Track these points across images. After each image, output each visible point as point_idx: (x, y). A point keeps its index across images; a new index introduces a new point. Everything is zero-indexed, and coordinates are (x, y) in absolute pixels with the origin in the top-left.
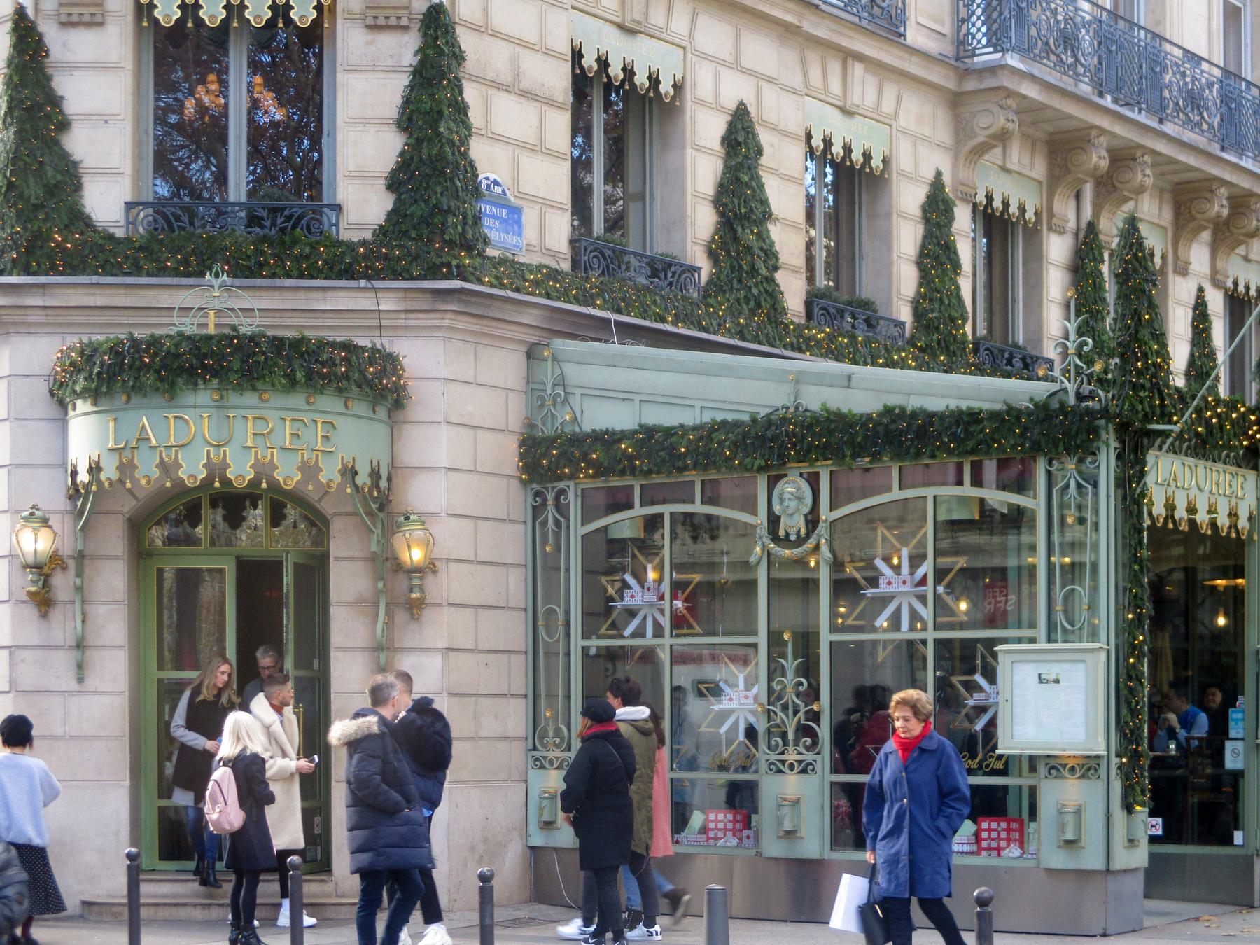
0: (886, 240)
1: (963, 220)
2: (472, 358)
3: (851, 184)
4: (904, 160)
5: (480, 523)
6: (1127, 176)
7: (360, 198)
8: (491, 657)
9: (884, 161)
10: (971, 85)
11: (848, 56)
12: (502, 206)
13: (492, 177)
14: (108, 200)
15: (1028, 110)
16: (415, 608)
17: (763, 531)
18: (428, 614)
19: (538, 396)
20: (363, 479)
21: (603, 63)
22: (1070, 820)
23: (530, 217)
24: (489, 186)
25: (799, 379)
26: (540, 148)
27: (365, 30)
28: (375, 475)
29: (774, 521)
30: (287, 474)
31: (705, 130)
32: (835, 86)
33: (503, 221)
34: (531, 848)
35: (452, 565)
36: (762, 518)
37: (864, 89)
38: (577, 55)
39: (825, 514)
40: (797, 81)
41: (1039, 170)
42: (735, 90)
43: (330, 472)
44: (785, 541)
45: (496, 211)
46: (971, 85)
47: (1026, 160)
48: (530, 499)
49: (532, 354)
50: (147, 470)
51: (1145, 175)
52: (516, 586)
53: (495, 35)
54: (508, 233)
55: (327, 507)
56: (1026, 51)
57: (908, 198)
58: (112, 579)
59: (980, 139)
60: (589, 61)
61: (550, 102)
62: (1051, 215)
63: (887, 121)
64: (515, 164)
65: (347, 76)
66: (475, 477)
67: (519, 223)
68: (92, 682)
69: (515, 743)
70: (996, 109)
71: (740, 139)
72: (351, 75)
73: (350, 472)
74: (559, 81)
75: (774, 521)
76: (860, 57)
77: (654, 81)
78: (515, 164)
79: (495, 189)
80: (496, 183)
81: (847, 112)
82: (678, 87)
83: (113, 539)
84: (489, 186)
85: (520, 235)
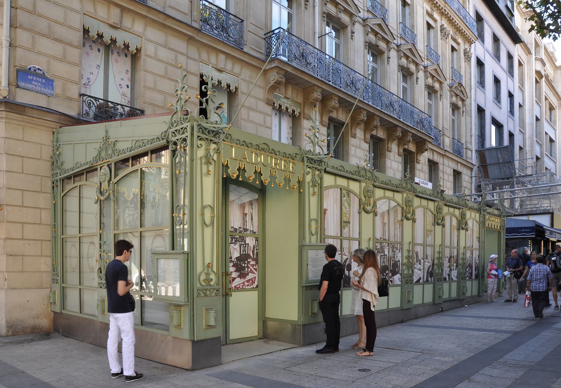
2: (22, 131)
6: (330, 103)
9: (236, 88)
12: (42, 78)
13: (37, 67)
24: (35, 70)
33: (42, 83)
40: (196, 56)
41: (300, 99)
47: (295, 96)
53: (40, 15)
59: (272, 84)
61: (71, 45)
62: (304, 113)
63: (238, 76)
64: (49, 64)
67: (52, 86)
70: (276, 74)
74: (77, 37)
78: (49, 64)
80: (39, 69)
81: (220, 71)
84: (35, 70)
85: (52, 90)
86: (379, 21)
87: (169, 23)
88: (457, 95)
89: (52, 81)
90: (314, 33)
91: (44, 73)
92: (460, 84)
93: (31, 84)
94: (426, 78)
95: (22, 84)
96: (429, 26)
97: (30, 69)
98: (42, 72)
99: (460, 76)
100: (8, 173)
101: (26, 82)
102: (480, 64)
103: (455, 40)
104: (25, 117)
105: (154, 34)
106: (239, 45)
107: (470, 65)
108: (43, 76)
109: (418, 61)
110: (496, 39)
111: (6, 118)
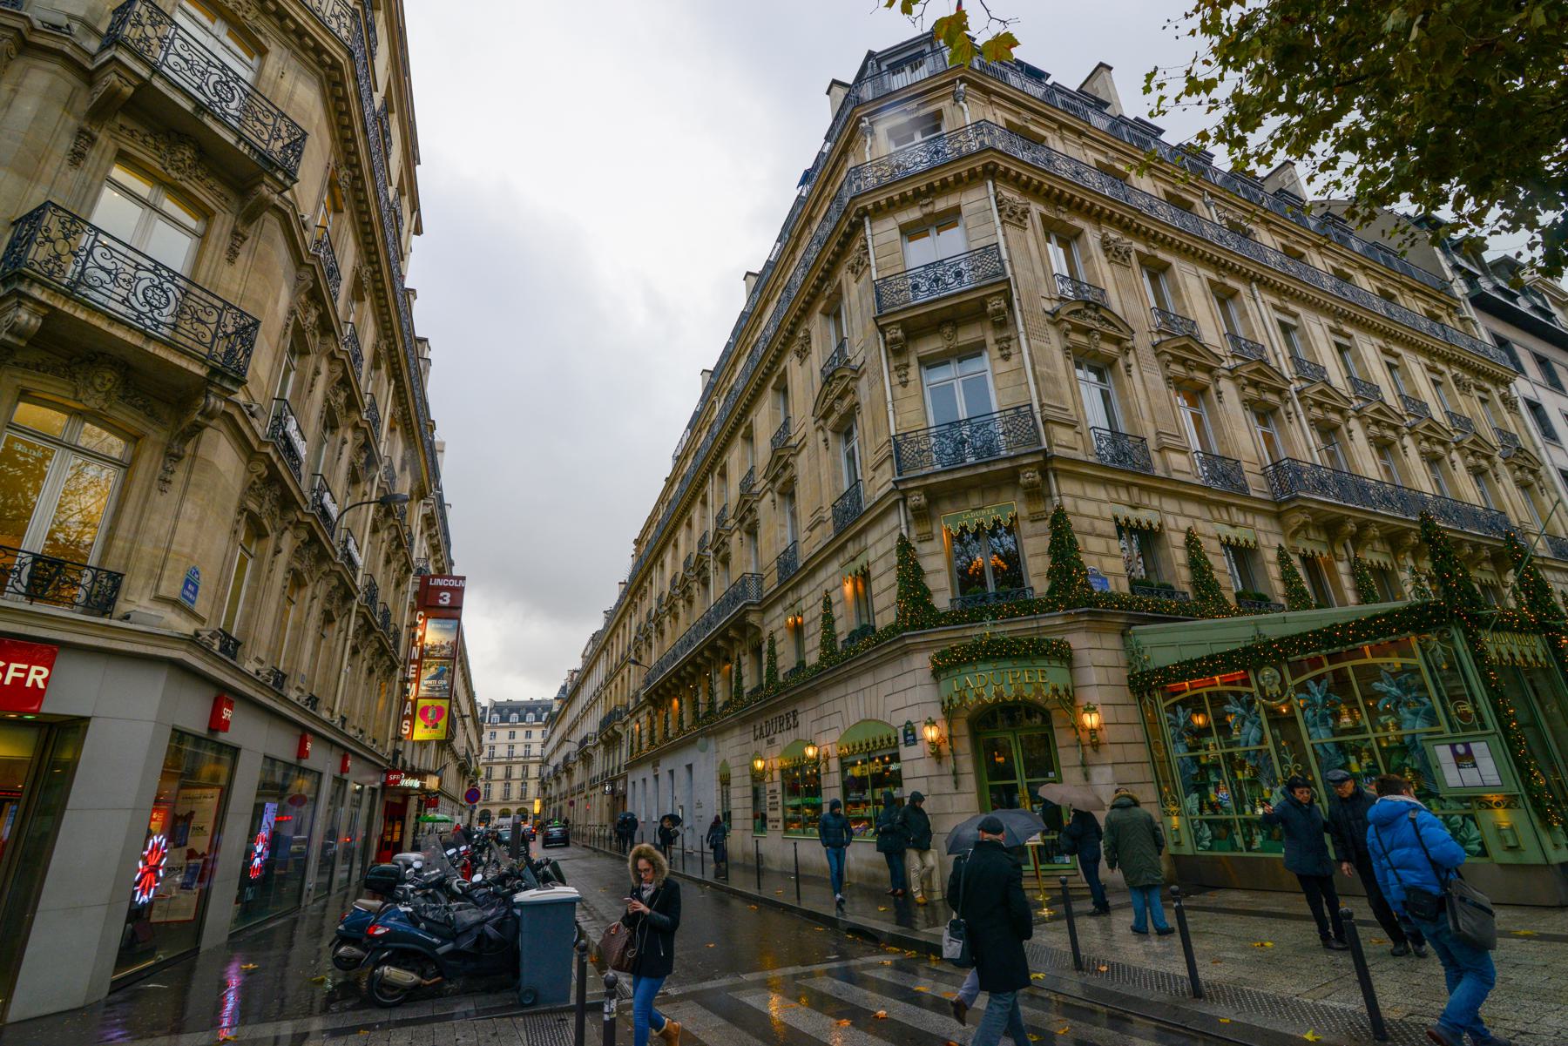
0: (1265, 572)
1: (1296, 561)
3: (1243, 555)
4: (1263, 540)
7: (1038, 585)
10: (1285, 508)
11: (1227, 506)
14: (942, 601)
15: (1313, 512)
17: (1257, 695)
19: (1133, 653)
20: (1062, 692)
21: (1127, 520)
22: (1508, 833)
23: (1111, 580)
25: (1256, 624)
26: (1109, 555)
28: (1067, 690)
29: (1262, 690)
30: (1029, 693)
31: (1178, 539)
32: (1226, 517)
36: (1254, 689)
37: (1238, 517)
38: (1116, 519)
39: (1290, 682)
40: (1208, 517)
42: (1184, 523)
43: (1047, 691)
44: (1271, 698)
46: (1285, 508)
49: (1123, 634)
50: (971, 698)
51: (1374, 531)
52: (1138, 733)
55: (1048, 706)
56: (1307, 490)
57: (1271, 555)
58: (965, 746)
60: (1122, 520)
61: (1109, 537)
63: (1252, 527)
68: (961, 789)
71: (1192, 542)
73: (1056, 690)
74: (1110, 528)
75: (1262, 690)
76: (1233, 505)
77: (1150, 524)
81: (1234, 526)
82: (1160, 525)
83: (962, 728)
86: (1376, 406)
87: (1181, 489)
88: (1521, 468)
90: (1310, 449)
92: (1520, 450)
94: (1464, 458)
96: (1436, 384)
99: (1514, 438)
102: (1535, 407)
103: (1479, 388)
105: (1170, 505)
106: (1243, 490)
107: (1522, 417)
109: (1446, 437)
110: (1542, 362)
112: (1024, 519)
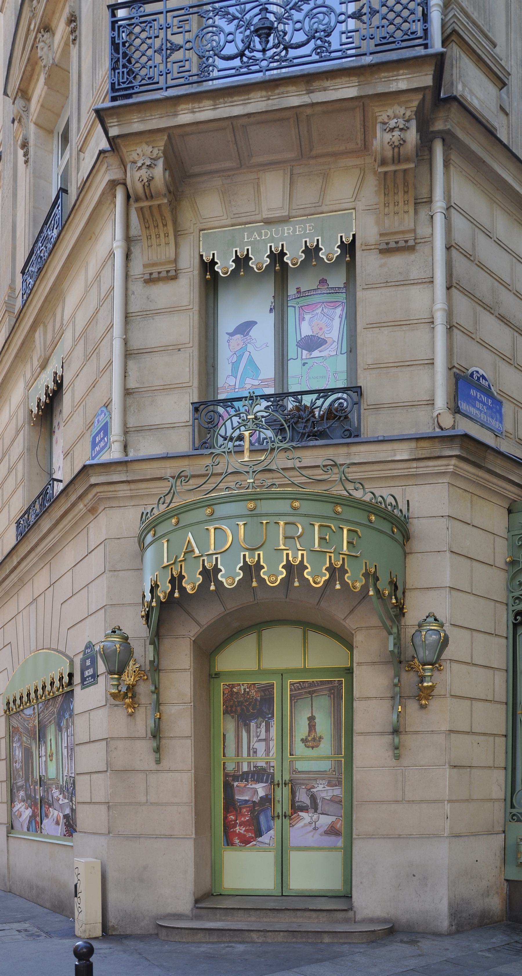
2: (469, 505)
5: (475, 634)
8: (481, 738)
13: (481, 372)
16: (424, 695)
18: (434, 704)
24: (479, 378)
27: (380, 256)
34: (507, 880)
35: (455, 666)
45: (485, 399)
48: (511, 618)
54: (493, 418)
65: (365, 292)
66: (472, 598)
69: (496, 804)
72: (369, 292)
79: (483, 382)
80: (483, 377)
84: (479, 378)
89: (500, 403)
91: (489, 385)
93: (474, 406)
95: (463, 406)
97: (472, 375)
98: (487, 383)
100: (453, 592)
101: (468, 403)
104: (481, 473)
108: (487, 392)
111: (454, 474)
112: (367, 248)
